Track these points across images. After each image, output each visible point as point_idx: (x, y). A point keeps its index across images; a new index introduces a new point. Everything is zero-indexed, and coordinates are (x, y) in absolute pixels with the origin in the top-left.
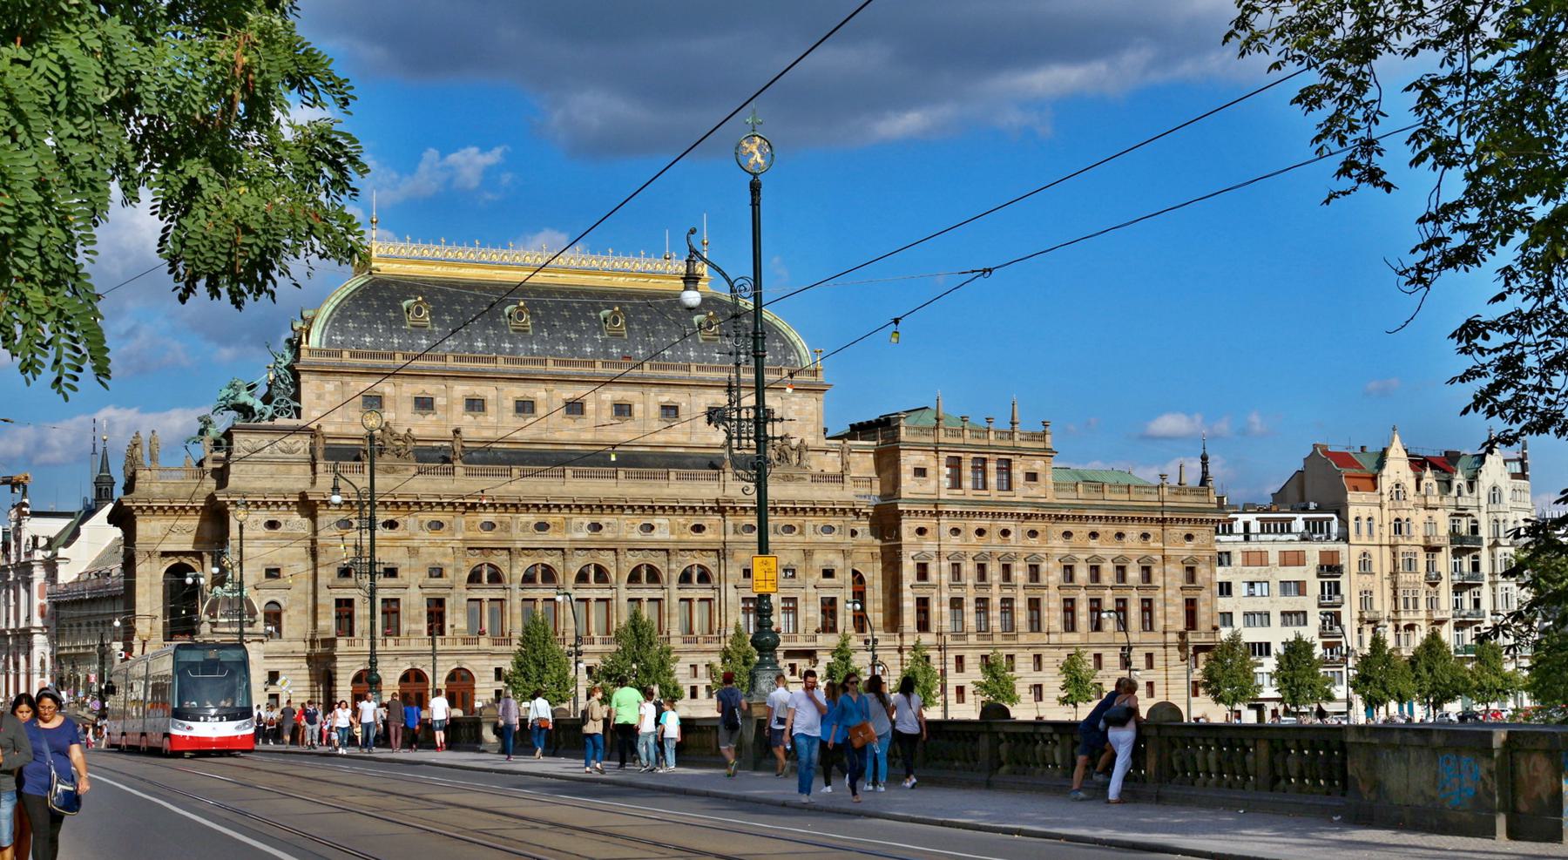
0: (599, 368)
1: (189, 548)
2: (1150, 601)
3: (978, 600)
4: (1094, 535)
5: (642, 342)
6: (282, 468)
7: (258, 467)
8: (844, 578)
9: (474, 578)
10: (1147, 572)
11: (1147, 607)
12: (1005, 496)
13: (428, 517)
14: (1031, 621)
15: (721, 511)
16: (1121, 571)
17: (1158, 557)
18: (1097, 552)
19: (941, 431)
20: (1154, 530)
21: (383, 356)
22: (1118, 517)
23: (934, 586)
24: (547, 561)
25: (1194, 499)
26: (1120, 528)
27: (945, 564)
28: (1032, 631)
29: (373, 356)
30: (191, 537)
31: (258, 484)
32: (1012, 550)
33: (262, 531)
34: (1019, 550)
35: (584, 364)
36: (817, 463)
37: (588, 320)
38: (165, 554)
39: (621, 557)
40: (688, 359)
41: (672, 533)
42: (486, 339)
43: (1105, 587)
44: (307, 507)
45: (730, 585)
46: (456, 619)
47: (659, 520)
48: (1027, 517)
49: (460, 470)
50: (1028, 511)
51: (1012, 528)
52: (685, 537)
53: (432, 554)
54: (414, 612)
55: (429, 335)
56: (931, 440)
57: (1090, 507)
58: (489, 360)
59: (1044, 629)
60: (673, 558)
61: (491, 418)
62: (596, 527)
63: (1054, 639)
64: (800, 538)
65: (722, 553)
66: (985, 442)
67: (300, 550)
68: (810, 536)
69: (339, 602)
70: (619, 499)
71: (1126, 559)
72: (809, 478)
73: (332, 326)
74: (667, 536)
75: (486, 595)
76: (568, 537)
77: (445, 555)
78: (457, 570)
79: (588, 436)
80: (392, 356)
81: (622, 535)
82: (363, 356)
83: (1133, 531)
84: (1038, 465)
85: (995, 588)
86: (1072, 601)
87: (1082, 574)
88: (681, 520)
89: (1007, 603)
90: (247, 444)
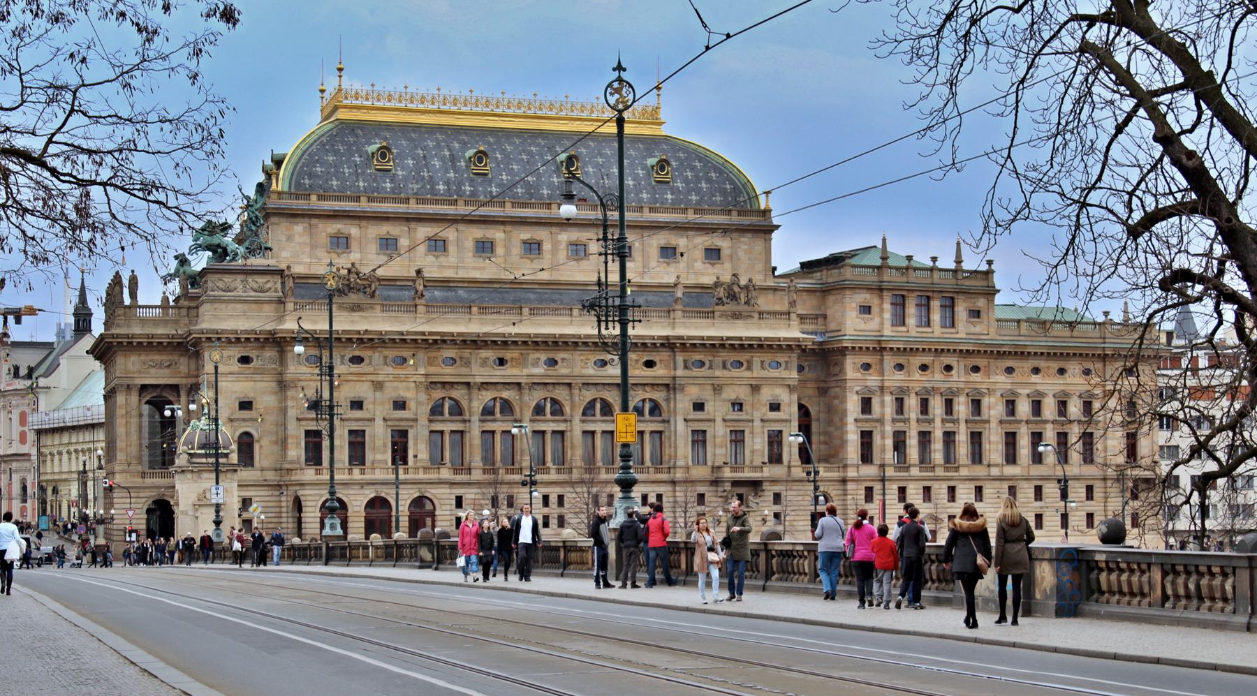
4: (1036, 371)
6: (254, 306)
7: (231, 306)
8: (790, 411)
9: (436, 411)
10: (1087, 406)
11: (1087, 438)
12: (949, 334)
14: (973, 454)
16: (1063, 405)
21: (349, 199)
22: (1060, 355)
27: (888, 399)
28: (974, 462)
29: (339, 198)
33: (236, 367)
34: (961, 385)
35: (541, 205)
38: (144, 388)
39: (576, 392)
43: (1046, 422)
45: (680, 419)
46: (419, 449)
53: (396, 388)
59: (985, 462)
61: (452, 259)
62: (553, 363)
63: (995, 472)
64: (747, 374)
65: (670, 387)
68: (757, 372)
69: (308, 433)
71: (1066, 394)
72: (756, 316)
75: (447, 427)
76: (525, 372)
77: (408, 389)
78: (419, 403)
80: (358, 199)
81: (577, 371)
82: (329, 198)
83: (1074, 368)
84: (981, 303)
86: (1014, 434)
87: (1024, 408)
89: (949, 437)
90: (221, 284)
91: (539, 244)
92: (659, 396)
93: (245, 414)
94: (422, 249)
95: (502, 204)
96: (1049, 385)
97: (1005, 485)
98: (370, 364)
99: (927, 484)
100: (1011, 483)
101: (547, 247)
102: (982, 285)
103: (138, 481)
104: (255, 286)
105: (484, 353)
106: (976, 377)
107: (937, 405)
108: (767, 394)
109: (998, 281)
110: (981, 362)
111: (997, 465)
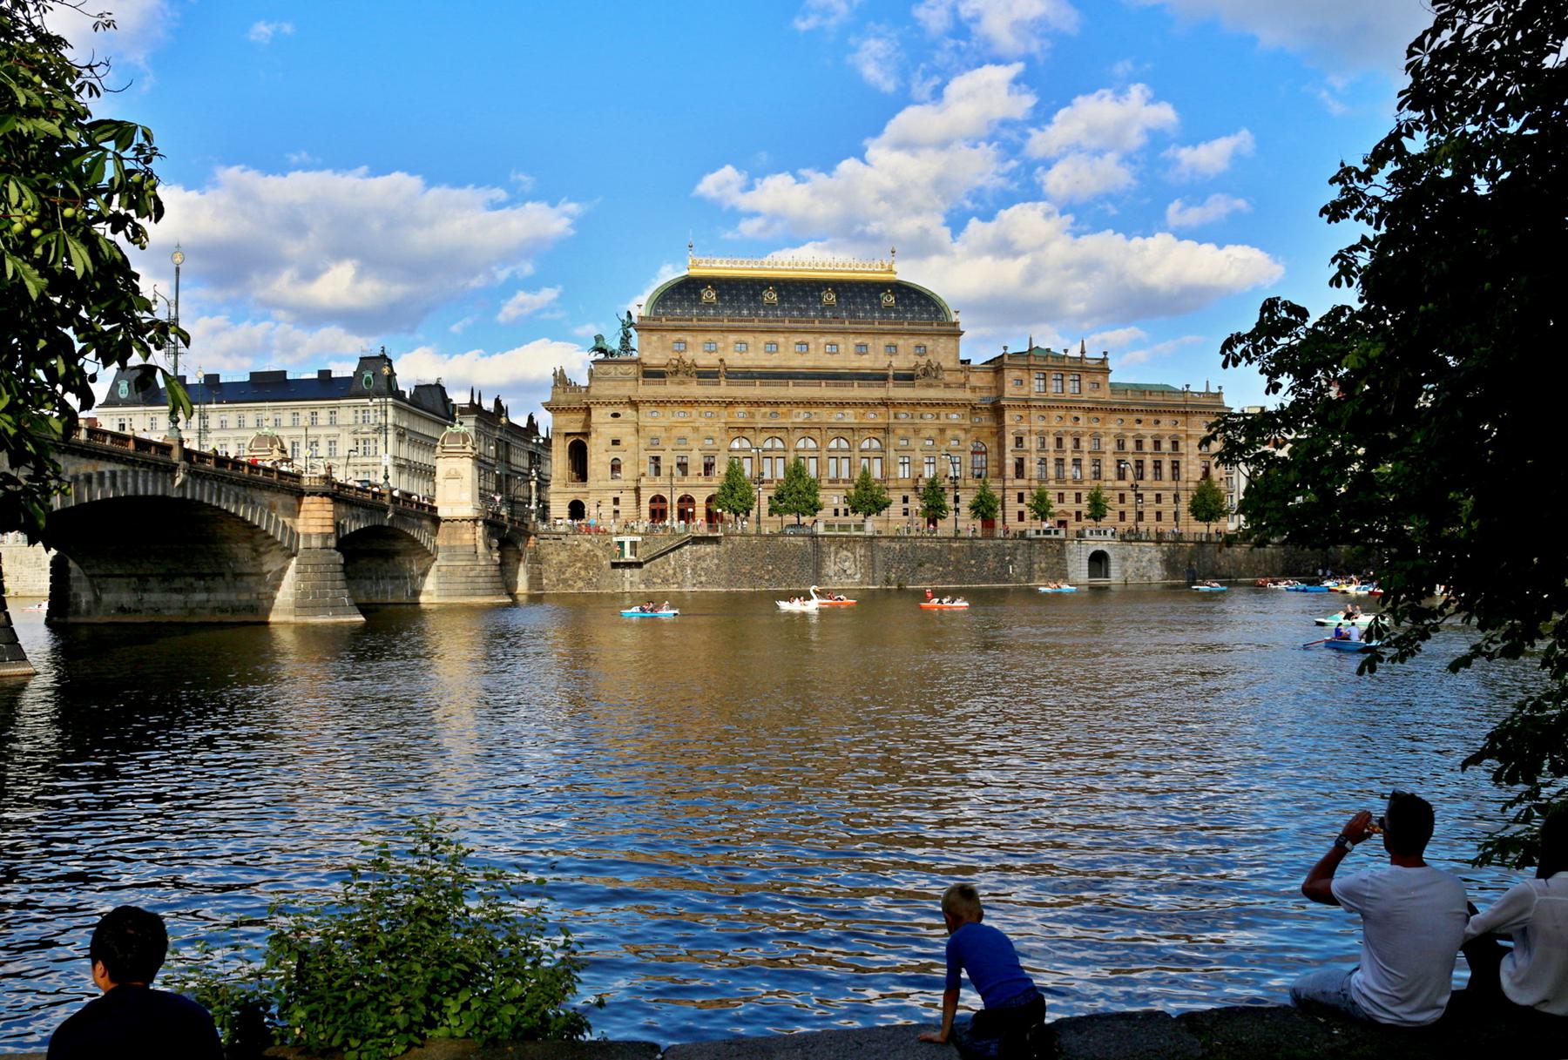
0: (817, 324)
4: (1139, 421)
10: (1175, 444)
11: (1176, 466)
13: (703, 410)
16: (1157, 444)
20: (1180, 419)
22: (1156, 411)
36: (947, 378)
38: (568, 434)
44: (634, 404)
48: (1090, 410)
55: (715, 308)
61: (751, 355)
63: (1109, 484)
67: (630, 429)
68: (943, 420)
79: (810, 364)
83: (1166, 421)
84: (1100, 378)
85: (1069, 453)
87: (1130, 445)
92: (880, 435)
96: (1148, 431)
97: (1117, 493)
101: (812, 346)
102: (1103, 368)
105: (763, 410)
107: (1068, 443)
108: (949, 433)
109: (1111, 365)
110: (1100, 415)
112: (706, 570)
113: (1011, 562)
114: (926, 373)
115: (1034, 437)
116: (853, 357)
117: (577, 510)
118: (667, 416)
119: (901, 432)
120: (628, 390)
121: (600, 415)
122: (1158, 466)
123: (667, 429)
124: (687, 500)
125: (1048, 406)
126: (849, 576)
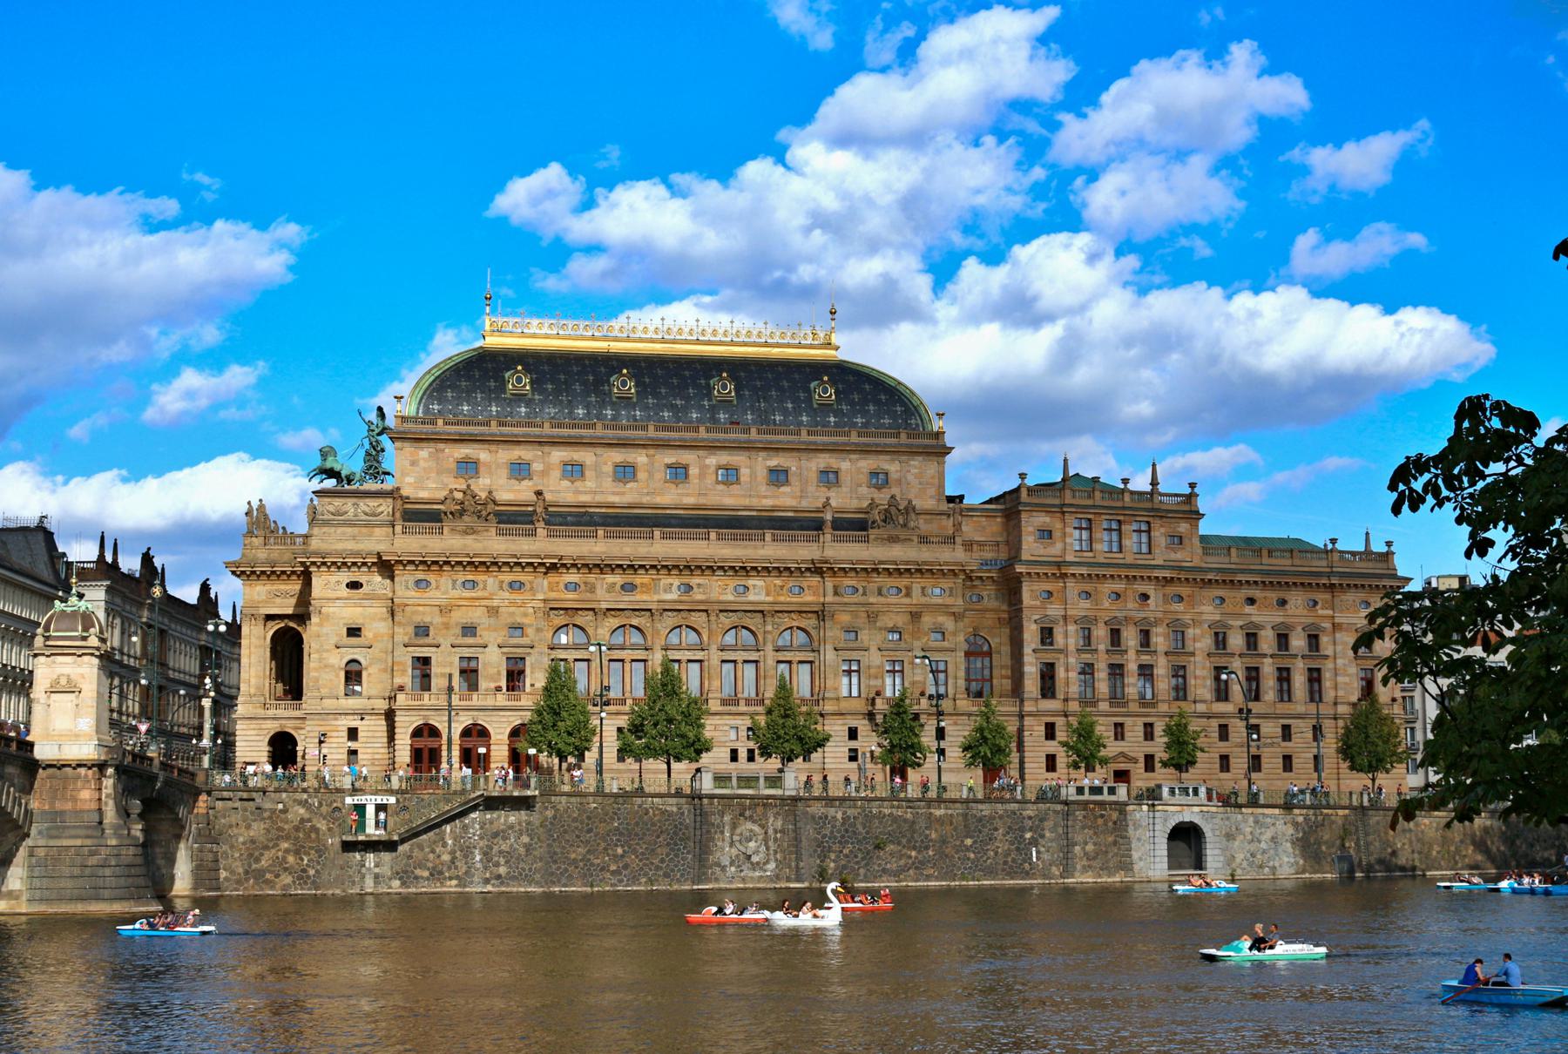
0: (703, 433)
1: (290, 611)
2: (1318, 670)
3: (1111, 666)
4: (1251, 601)
5: (752, 408)
6: (364, 530)
7: (340, 530)
10: (1313, 640)
11: (1315, 677)
13: (507, 577)
15: (818, 571)
16: (1283, 639)
17: (1327, 625)
18: (1254, 619)
19: (1068, 492)
20: (1322, 596)
22: (1280, 583)
23: (1060, 651)
24: (635, 622)
25: (1371, 565)
26: (1282, 594)
30: (293, 601)
31: (340, 546)
32: (1151, 616)
33: (345, 592)
34: (1160, 615)
35: (687, 430)
36: (924, 526)
37: (696, 386)
38: (269, 618)
39: (713, 618)
40: (800, 424)
41: (768, 594)
42: (587, 406)
43: (1265, 656)
44: (386, 567)
45: (829, 647)
47: (755, 582)
48: (1168, 581)
49: (541, 532)
50: (1168, 574)
51: (1151, 593)
52: (782, 599)
53: (513, 614)
54: (493, 671)
55: (529, 403)
56: (1057, 502)
57: (1251, 572)
58: (588, 426)
59: (1190, 697)
60: (769, 619)
61: (590, 484)
63: (1201, 708)
64: (907, 601)
66: (1119, 504)
67: (381, 610)
68: (916, 597)
70: (707, 560)
71: (1290, 627)
72: (915, 539)
73: (430, 396)
74: (762, 598)
76: (656, 598)
77: (525, 615)
78: (538, 630)
79: (691, 501)
80: (488, 424)
83: (1297, 600)
84: (1183, 527)
85: (1131, 655)
87: (1236, 641)
88: (778, 582)
90: (331, 508)
91: (686, 468)
92: (810, 623)
93: (354, 640)
94: (556, 473)
95: (645, 428)
96: (1266, 618)
97: (1215, 723)
98: (485, 588)
99: (1119, 720)
100: (1223, 721)
101: (694, 471)
102: (1188, 508)
103: (261, 712)
104: (367, 510)
105: (610, 578)
106: (1180, 607)
107: (1130, 638)
108: (927, 620)
109: (1202, 504)
110: (1184, 591)
111: (1204, 701)
112: (508, 855)
113: (1034, 842)
114: (888, 518)
115: (1072, 628)
116: (763, 489)
117: (283, 749)
118: (445, 587)
119: (845, 618)
120: (378, 542)
121: (326, 585)
122: (1284, 676)
123: (444, 610)
124: (476, 733)
125: (1096, 574)
126: (755, 866)
